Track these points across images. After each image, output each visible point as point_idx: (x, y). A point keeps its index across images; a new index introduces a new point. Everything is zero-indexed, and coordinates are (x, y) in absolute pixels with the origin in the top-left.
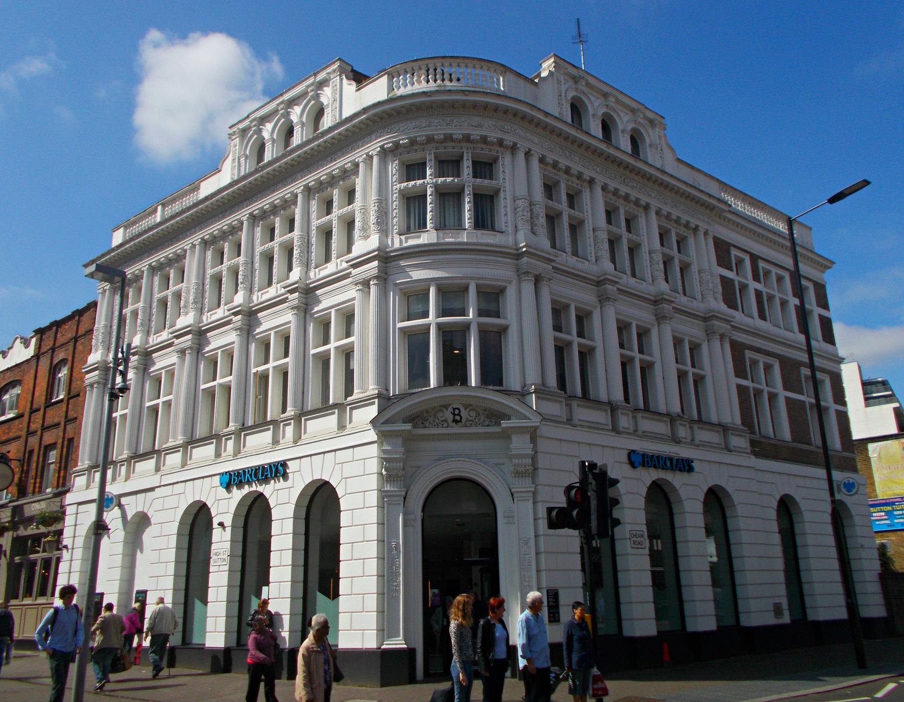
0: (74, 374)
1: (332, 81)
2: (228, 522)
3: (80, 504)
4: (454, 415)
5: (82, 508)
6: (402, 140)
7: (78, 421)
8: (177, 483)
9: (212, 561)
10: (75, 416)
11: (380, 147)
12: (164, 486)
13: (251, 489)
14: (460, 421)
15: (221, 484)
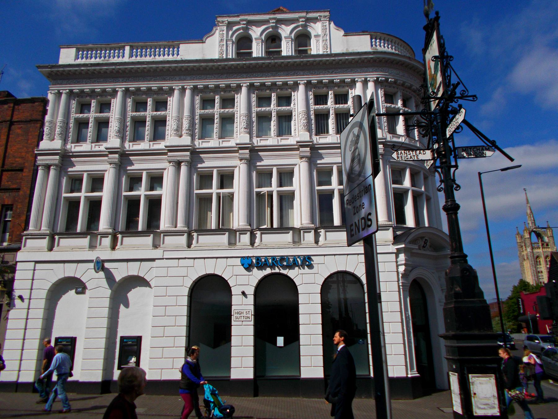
0: (9, 150)
1: (322, 22)
2: (250, 291)
3: (37, 262)
4: (425, 243)
5: (38, 266)
6: (391, 78)
7: (21, 192)
8: (185, 258)
9: (233, 318)
10: (15, 186)
11: (376, 77)
12: (166, 259)
13: (273, 271)
14: (425, 247)
15: (243, 265)
